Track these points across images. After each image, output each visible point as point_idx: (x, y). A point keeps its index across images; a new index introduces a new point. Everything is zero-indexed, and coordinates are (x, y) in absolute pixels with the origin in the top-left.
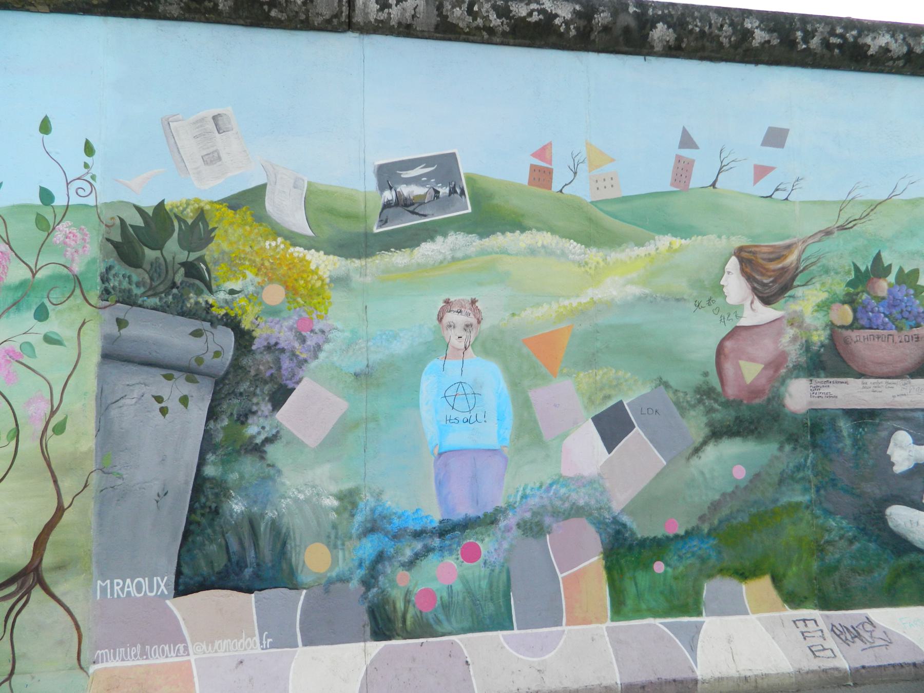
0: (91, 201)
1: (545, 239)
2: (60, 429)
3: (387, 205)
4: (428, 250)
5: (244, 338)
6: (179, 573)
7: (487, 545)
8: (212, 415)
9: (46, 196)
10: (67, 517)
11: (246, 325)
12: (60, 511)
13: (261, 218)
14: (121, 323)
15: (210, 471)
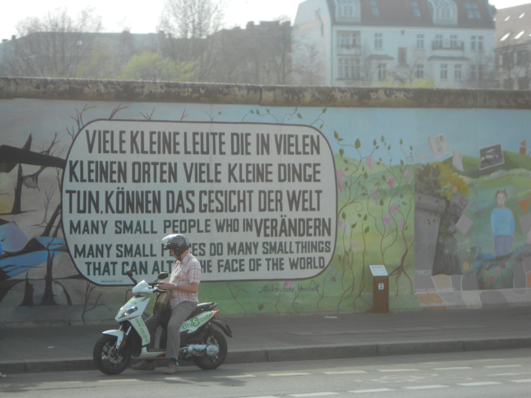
0: (412, 163)
1: (523, 171)
2: (406, 228)
3: (483, 162)
4: (494, 175)
5: (448, 203)
6: (434, 269)
7: (508, 264)
8: (441, 225)
9: (402, 162)
10: (408, 253)
11: (448, 199)
12: (407, 251)
13: (452, 166)
14: (419, 199)
15: (441, 241)
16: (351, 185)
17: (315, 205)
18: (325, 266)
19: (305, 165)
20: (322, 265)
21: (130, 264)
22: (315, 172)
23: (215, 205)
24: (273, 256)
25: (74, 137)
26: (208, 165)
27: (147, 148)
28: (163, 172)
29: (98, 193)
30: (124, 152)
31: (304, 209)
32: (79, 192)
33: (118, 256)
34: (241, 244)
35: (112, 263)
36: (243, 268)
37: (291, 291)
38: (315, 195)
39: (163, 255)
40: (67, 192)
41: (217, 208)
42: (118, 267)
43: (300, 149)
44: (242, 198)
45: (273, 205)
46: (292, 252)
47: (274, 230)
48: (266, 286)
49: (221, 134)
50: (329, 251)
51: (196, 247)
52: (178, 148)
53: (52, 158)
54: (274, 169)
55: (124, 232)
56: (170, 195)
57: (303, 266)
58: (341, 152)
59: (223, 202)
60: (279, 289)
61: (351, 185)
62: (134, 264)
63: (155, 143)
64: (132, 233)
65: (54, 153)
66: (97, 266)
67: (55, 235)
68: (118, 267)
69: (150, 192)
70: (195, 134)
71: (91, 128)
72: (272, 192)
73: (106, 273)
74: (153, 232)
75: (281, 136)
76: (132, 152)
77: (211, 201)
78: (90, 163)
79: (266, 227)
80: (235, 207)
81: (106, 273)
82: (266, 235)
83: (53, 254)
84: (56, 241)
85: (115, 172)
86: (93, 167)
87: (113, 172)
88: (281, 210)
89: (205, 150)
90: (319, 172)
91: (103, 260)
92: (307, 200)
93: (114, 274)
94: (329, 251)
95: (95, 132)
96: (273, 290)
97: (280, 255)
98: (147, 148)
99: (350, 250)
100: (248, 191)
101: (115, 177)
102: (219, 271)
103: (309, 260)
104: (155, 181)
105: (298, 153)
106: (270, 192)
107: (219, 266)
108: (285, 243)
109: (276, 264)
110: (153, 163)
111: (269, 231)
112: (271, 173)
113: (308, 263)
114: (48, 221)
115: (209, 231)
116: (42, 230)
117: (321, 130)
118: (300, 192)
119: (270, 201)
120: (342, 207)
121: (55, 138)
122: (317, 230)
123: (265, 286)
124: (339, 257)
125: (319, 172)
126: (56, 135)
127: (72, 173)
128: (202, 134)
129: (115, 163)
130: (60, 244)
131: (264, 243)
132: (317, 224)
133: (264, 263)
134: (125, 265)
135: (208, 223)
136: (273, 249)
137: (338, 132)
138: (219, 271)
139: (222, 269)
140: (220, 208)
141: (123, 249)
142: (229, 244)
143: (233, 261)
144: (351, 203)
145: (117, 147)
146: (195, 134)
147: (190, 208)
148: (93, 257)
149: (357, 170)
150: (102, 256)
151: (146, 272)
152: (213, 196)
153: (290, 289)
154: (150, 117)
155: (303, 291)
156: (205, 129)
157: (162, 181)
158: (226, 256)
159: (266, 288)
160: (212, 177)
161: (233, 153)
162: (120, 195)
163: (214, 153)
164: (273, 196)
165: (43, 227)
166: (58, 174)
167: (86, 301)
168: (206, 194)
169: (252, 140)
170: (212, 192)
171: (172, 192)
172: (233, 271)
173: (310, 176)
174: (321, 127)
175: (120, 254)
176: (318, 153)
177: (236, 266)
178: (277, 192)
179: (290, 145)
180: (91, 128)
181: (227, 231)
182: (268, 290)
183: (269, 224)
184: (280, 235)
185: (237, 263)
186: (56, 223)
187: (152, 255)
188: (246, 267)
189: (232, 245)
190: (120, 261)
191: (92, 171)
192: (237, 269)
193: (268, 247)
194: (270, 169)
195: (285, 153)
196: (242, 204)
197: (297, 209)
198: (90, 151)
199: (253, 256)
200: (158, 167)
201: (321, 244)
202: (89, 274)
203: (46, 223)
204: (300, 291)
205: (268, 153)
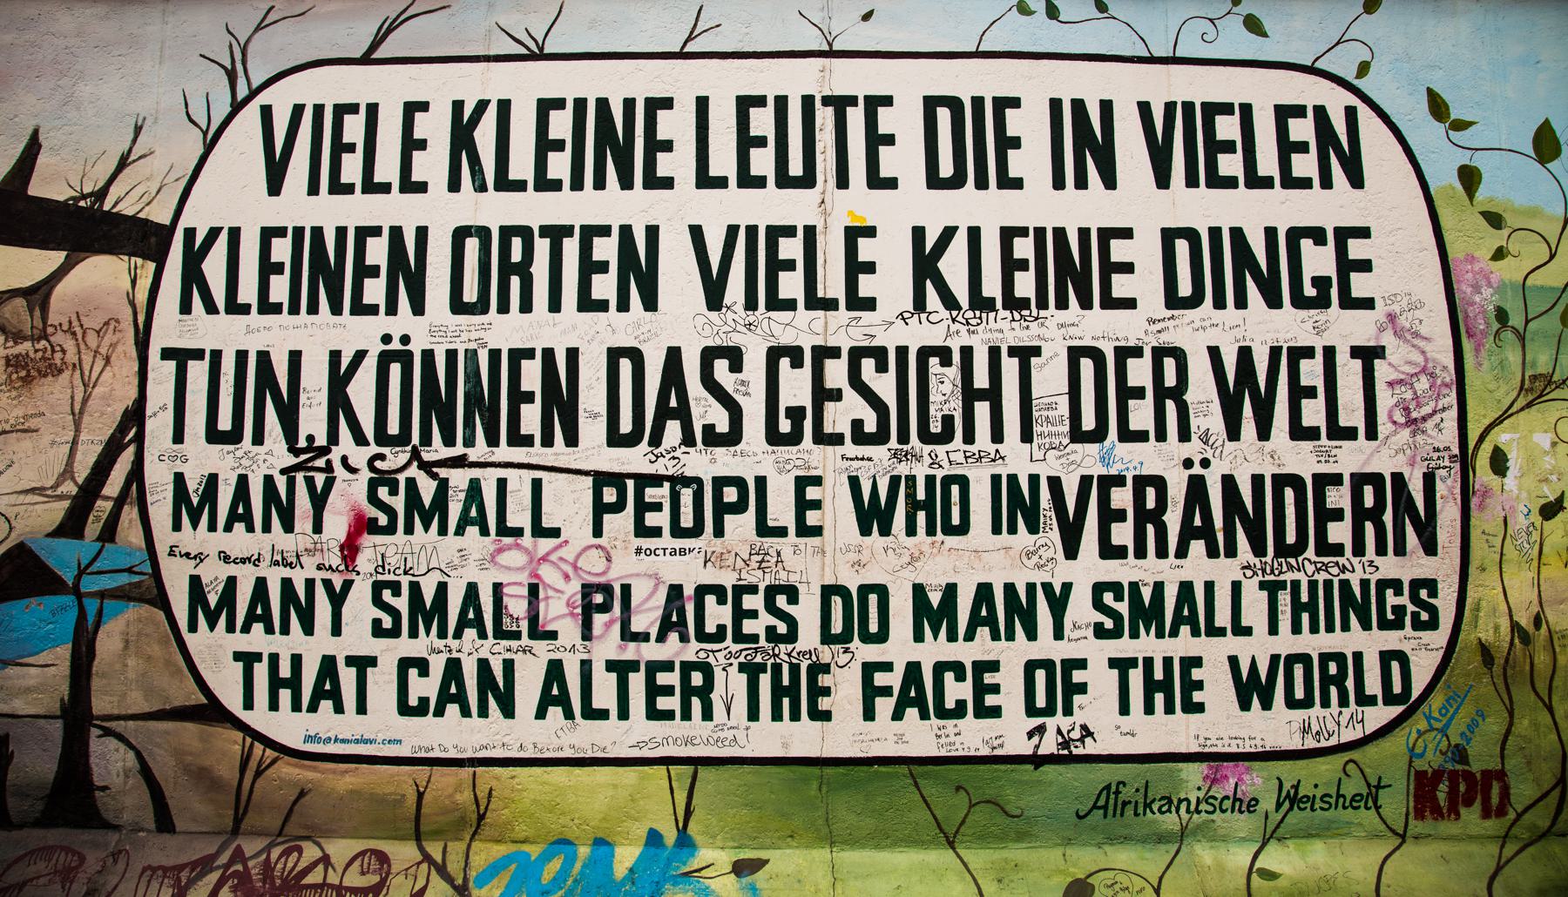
16: (1527, 322)
17: (1351, 414)
18: (1415, 694)
19: (1295, 234)
20: (1397, 688)
21: (437, 666)
22: (1347, 266)
23: (846, 412)
24: (1147, 645)
25: (210, 136)
26: (810, 231)
27: (522, 165)
28: (590, 267)
29: (295, 358)
30: (422, 188)
31: (1299, 432)
32: (217, 355)
33: (378, 630)
34: (984, 592)
35: (351, 661)
36: (990, 700)
37: (1241, 812)
38: (1349, 373)
39: (587, 634)
40: (167, 354)
41: (857, 424)
42: (382, 684)
43: (1268, 163)
44: (981, 380)
45: (1141, 415)
46: (1242, 631)
47: (1150, 529)
48: (1113, 788)
49: (876, 103)
50: (1433, 624)
51: (751, 602)
52: (665, 165)
53: (116, 219)
54: (1143, 252)
55: (409, 530)
56: (625, 366)
57: (1299, 693)
58: (1469, 178)
59: (890, 398)
60: (1180, 801)
61: (1527, 322)
62: (453, 669)
63: (559, 145)
64: (443, 531)
65: (126, 200)
66: (285, 671)
67: (109, 533)
68: (382, 684)
69: (529, 354)
70: (746, 104)
71: (281, 99)
72: (1137, 352)
73: (326, 705)
74: (539, 531)
75: (1170, 107)
76: (454, 185)
77: (823, 394)
78: (268, 234)
79: (1109, 516)
80: (948, 421)
81: (326, 705)
82: (1109, 551)
83: (100, 613)
84: (112, 557)
85: (374, 272)
86: (281, 250)
87: (365, 271)
88: (1184, 435)
89: (796, 168)
90: (1365, 266)
91: (314, 648)
92: (1311, 392)
93: (362, 709)
94: (1433, 624)
95: (298, 110)
96: (1148, 805)
97: (1183, 644)
98: (522, 165)
99: (1537, 621)
100: (1013, 351)
101: (375, 291)
102: (869, 714)
103: (1333, 668)
104: (555, 305)
105: (1256, 181)
106: (1126, 353)
107: (871, 693)
108: (1209, 587)
109: (1166, 686)
110: (546, 231)
111: (1122, 534)
112: (1128, 268)
113: (1326, 680)
114: (82, 472)
115: (817, 531)
116: (58, 510)
117: (1359, 83)
118: (1275, 352)
119: (1128, 393)
120: (1487, 422)
121: (134, 141)
122: (1369, 528)
123: (1108, 787)
124: (1485, 651)
125: (1365, 266)
126: (138, 130)
127: (193, 276)
128: (781, 103)
129: (376, 231)
130: (130, 570)
131: (1099, 589)
132: (1369, 501)
133: (1100, 681)
134: (413, 673)
135: (812, 493)
136: (1147, 613)
137: (1446, 96)
138: (869, 714)
139: (885, 706)
140: (870, 426)
141: (402, 604)
142: (919, 591)
143: (940, 668)
144: (1522, 409)
145: (387, 168)
146: (746, 104)
147: (723, 427)
148: (269, 630)
149: (1552, 257)
150: (308, 629)
151: (508, 711)
152: (836, 373)
153: (1235, 799)
154: (541, 44)
155: (1306, 808)
156: (797, 80)
157: (587, 303)
158: (900, 648)
159: (1112, 796)
160: (832, 283)
161: (934, 181)
162: (395, 370)
163: (843, 182)
164: (1140, 372)
165: (61, 497)
166: (134, 282)
167: (238, 821)
168: (797, 363)
169: (1030, 124)
170: (834, 353)
171: (636, 356)
172: (942, 713)
173: (1321, 283)
174: (1363, 69)
175: (387, 622)
176: (1357, 181)
177: (958, 691)
178: (1159, 353)
179: (1217, 147)
180: (281, 99)
181: (911, 530)
182: (1125, 804)
183: (1122, 498)
184: (1182, 552)
185: (960, 677)
186: (113, 486)
187: (537, 632)
188: (1010, 696)
189: (935, 598)
190: (389, 652)
191: (279, 268)
192: (961, 705)
193: (1123, 608)
194: (1120, 251)
195: (1192, 181)
196: (982, 410)
197: (1264, 433)
198: (275, 187)
199: (1046, 647)
200: (571, 247)
201: (1389, 592)
202: (249, 704)
203: (76, 483)
204: (1291, 808)
205: (1110, 182)
